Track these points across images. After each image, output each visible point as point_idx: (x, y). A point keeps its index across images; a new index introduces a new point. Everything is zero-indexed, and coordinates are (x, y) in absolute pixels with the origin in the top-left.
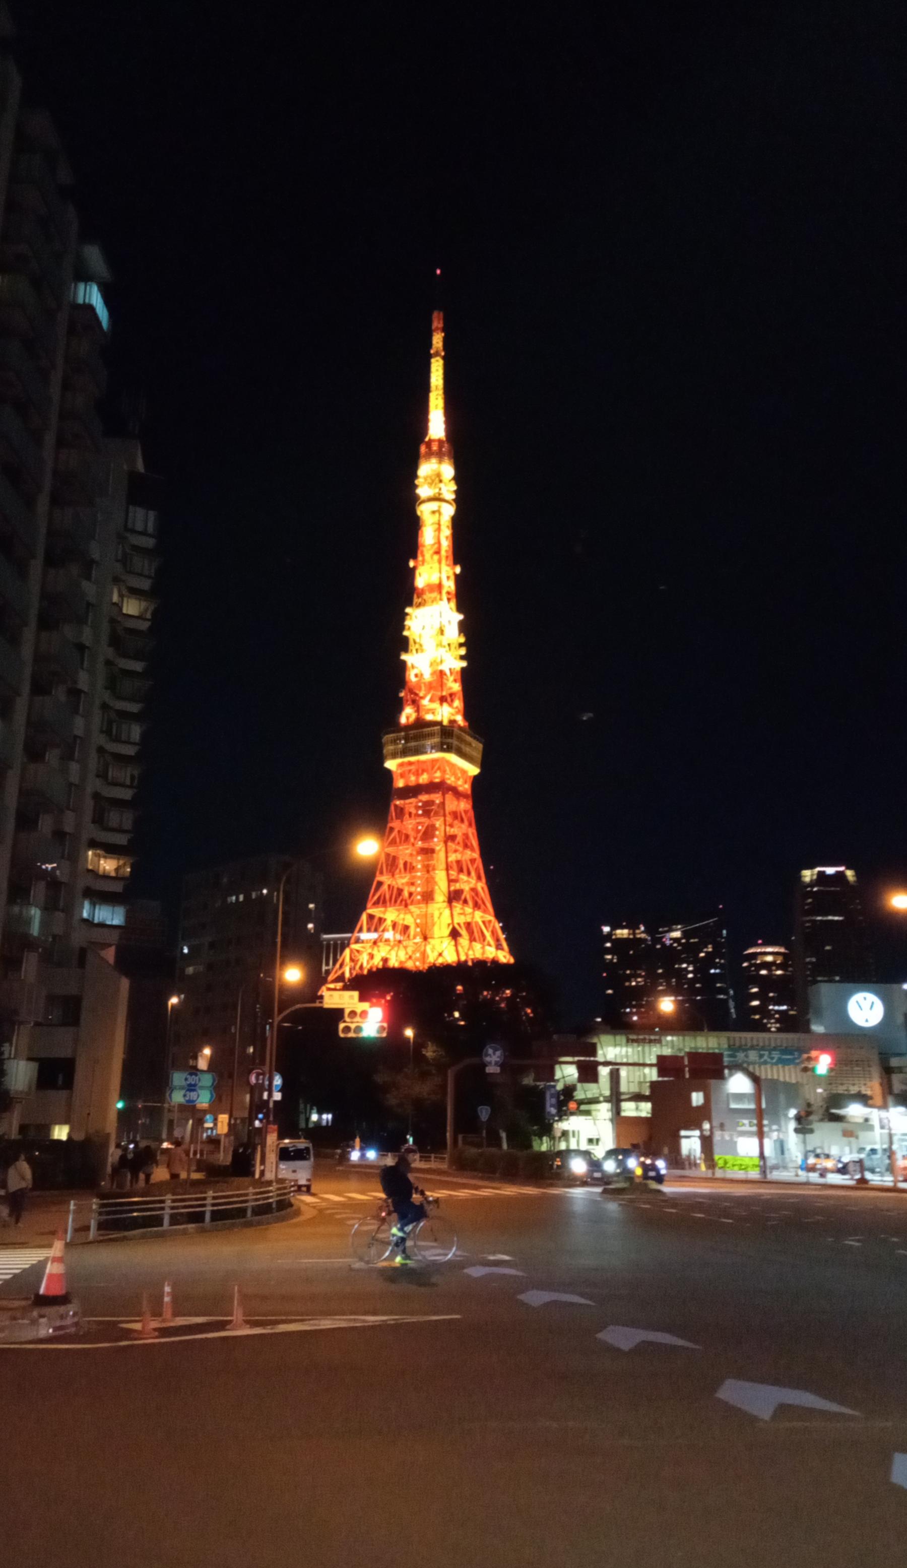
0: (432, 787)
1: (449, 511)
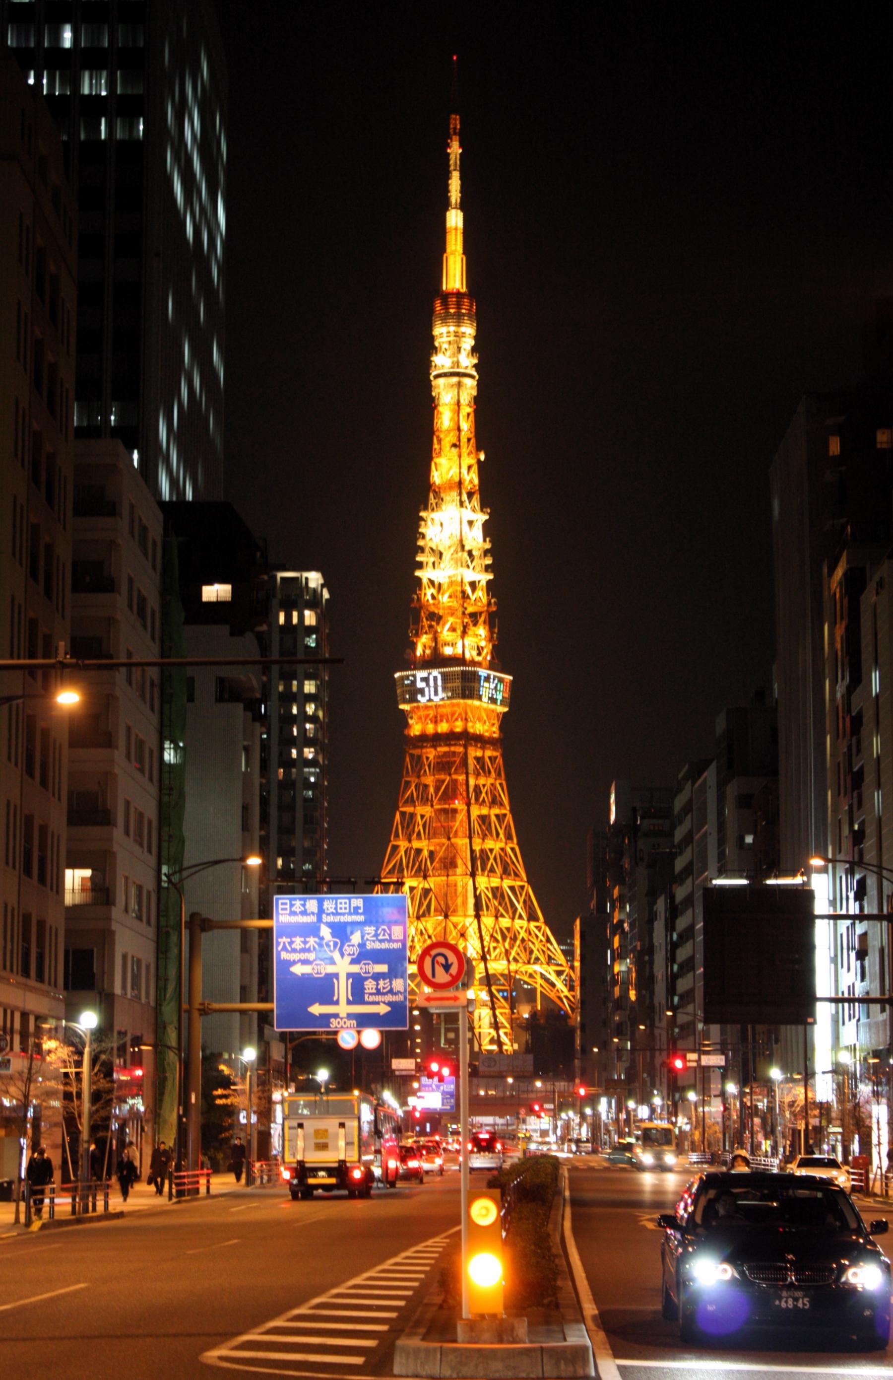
0: (450, 737)
1: (470, 386)
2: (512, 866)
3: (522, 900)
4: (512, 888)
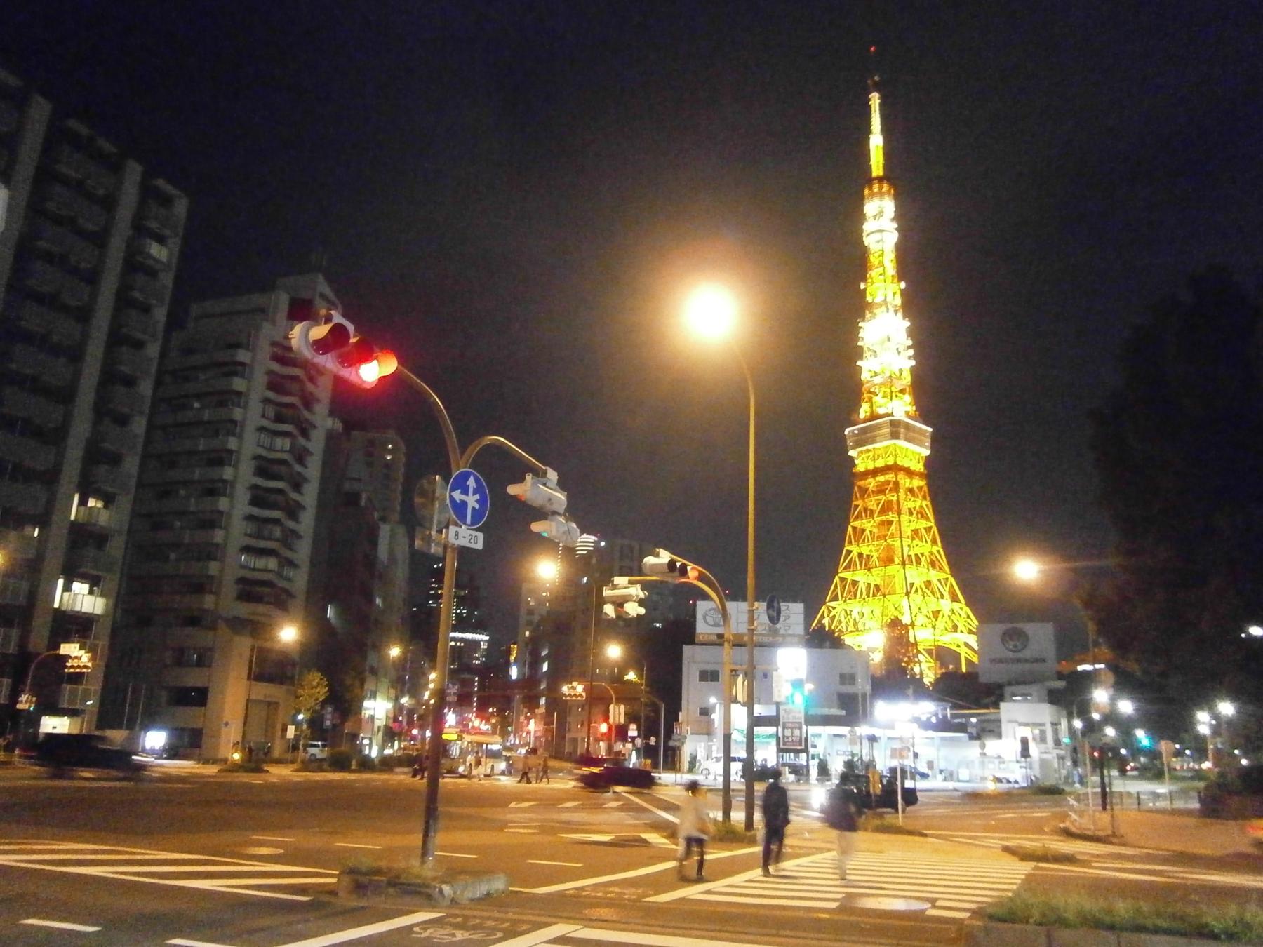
0: (886, 469)
2: (937, 563)
3: (947, 589)
4: (939, 581)
